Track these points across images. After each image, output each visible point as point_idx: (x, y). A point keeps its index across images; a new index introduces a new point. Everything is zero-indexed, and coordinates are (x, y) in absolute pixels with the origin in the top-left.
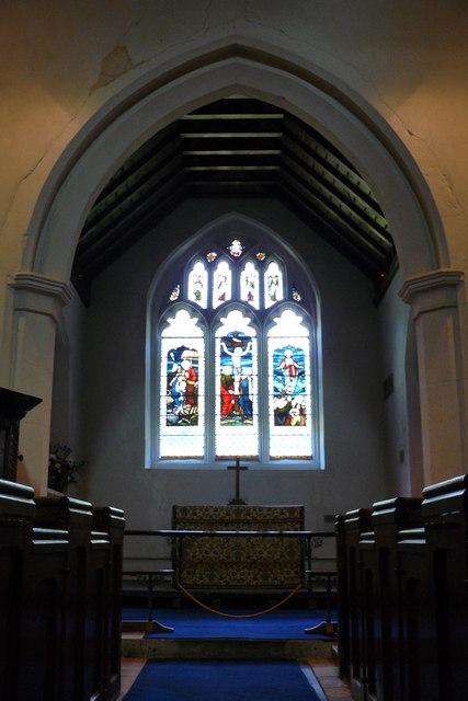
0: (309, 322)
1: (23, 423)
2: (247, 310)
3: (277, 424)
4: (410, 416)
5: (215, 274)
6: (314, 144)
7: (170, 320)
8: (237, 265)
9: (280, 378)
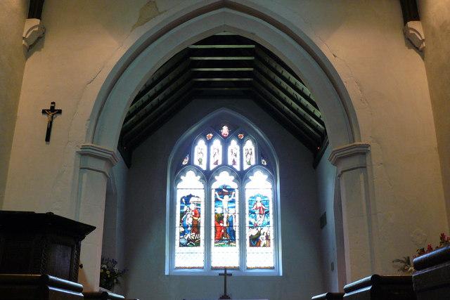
0: (272, 178)
1: (83, 243)
2: (232, 171)
3: (251, 245)
4: (337, 239)
5: (212, 148)
6: (274, 64)
7: (182, 177)
8: (226, 142)
9: (253, 215)
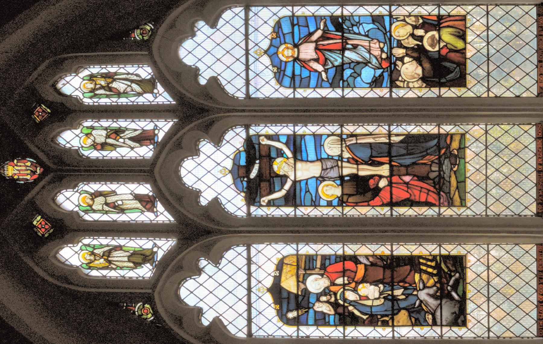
2: (178, 147)
